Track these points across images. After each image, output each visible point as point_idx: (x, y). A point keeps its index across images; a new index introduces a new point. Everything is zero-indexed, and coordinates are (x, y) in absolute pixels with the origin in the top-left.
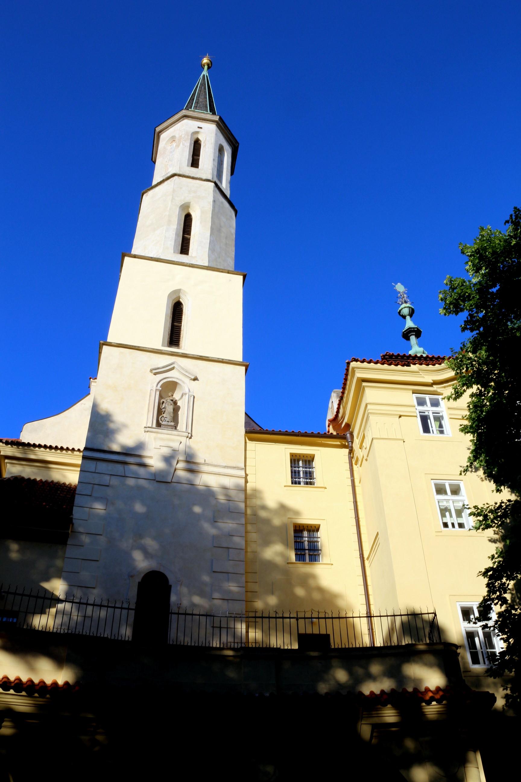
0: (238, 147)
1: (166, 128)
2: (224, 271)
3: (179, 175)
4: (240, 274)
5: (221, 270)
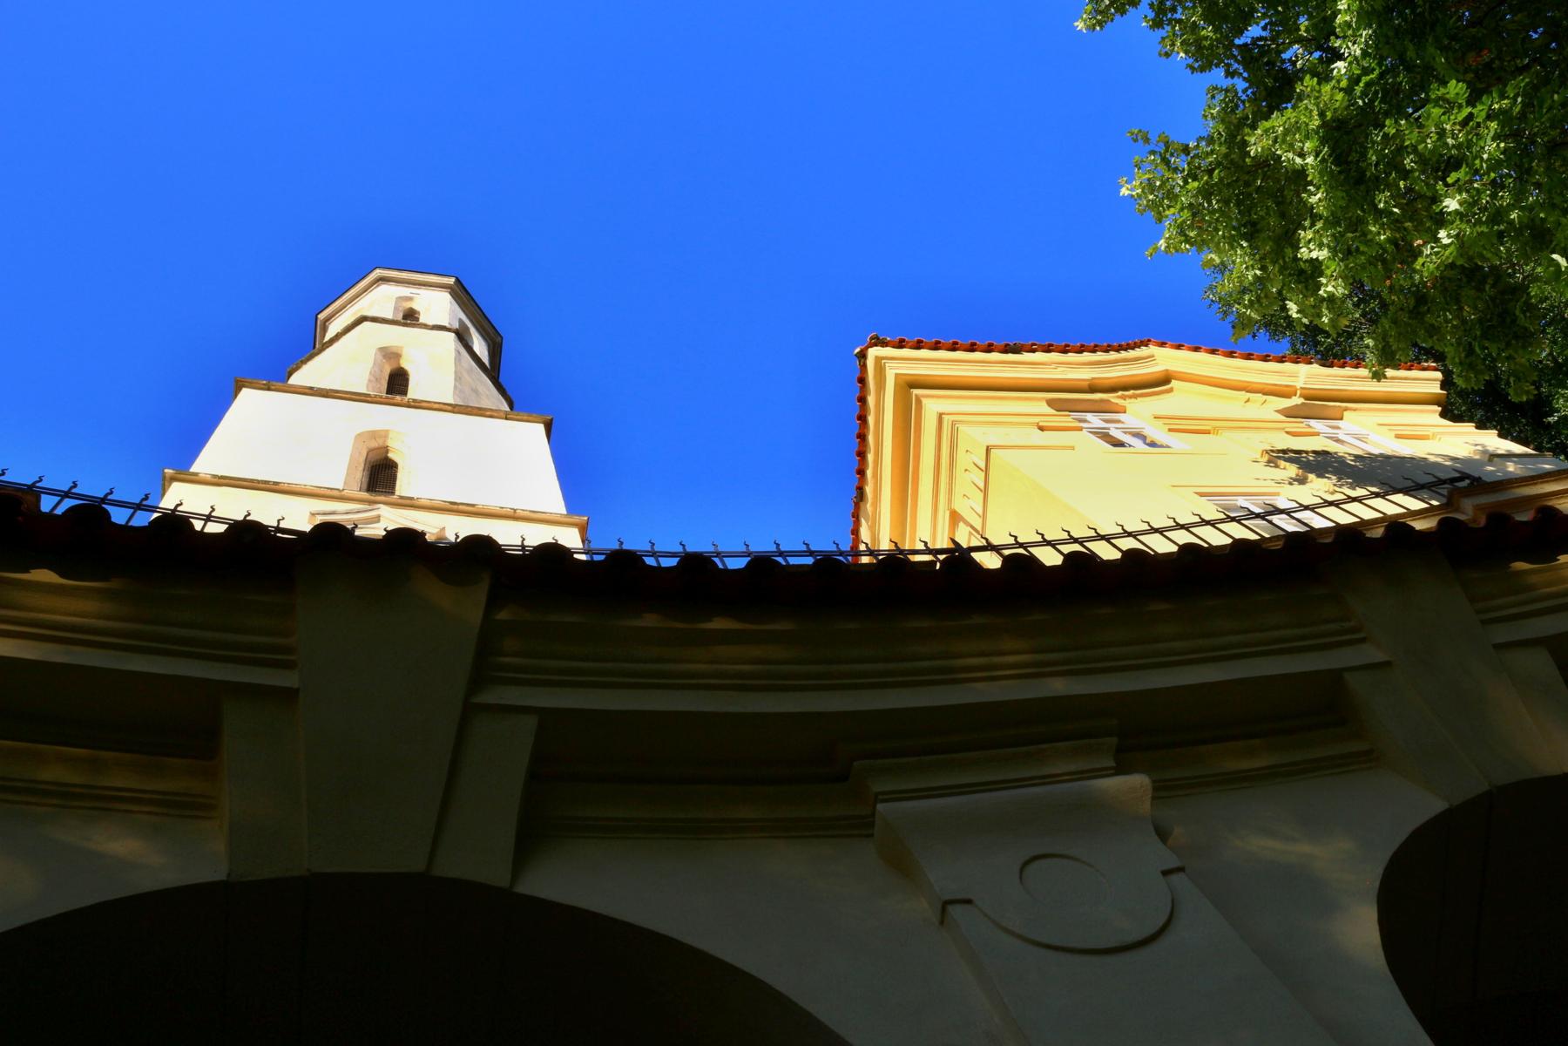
0: (501, 346)
1: (341, 310)
2: (495, 414)
3: (374, 320)
4: (536, 420)
5: (488, 413)
